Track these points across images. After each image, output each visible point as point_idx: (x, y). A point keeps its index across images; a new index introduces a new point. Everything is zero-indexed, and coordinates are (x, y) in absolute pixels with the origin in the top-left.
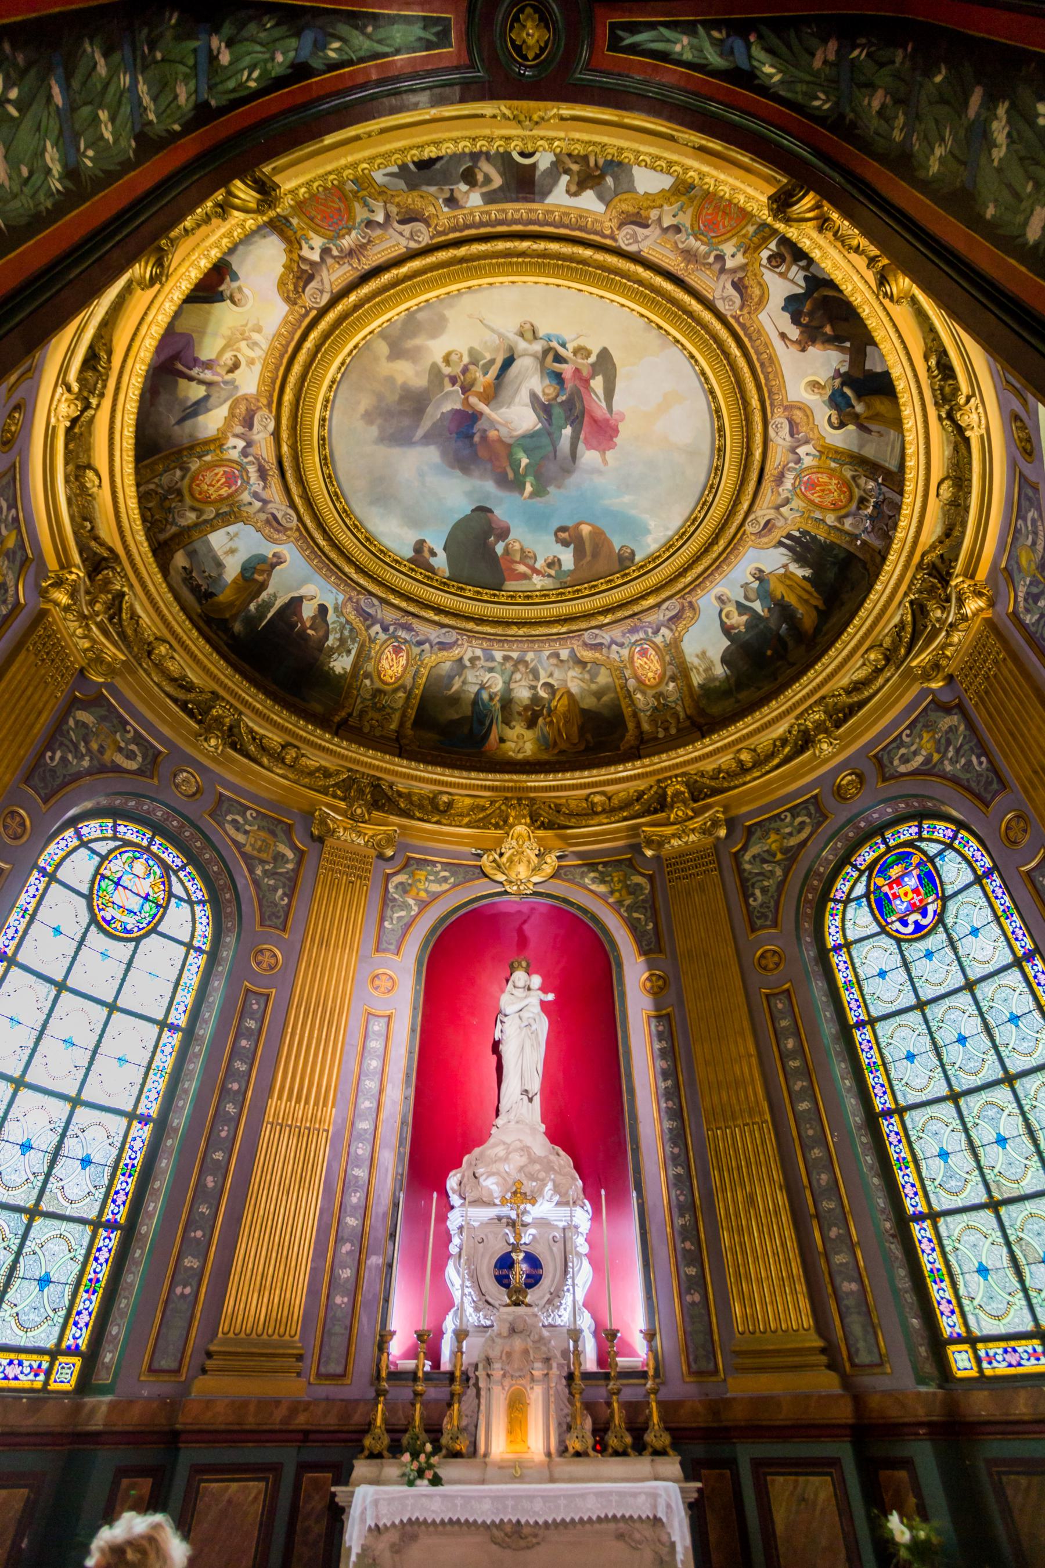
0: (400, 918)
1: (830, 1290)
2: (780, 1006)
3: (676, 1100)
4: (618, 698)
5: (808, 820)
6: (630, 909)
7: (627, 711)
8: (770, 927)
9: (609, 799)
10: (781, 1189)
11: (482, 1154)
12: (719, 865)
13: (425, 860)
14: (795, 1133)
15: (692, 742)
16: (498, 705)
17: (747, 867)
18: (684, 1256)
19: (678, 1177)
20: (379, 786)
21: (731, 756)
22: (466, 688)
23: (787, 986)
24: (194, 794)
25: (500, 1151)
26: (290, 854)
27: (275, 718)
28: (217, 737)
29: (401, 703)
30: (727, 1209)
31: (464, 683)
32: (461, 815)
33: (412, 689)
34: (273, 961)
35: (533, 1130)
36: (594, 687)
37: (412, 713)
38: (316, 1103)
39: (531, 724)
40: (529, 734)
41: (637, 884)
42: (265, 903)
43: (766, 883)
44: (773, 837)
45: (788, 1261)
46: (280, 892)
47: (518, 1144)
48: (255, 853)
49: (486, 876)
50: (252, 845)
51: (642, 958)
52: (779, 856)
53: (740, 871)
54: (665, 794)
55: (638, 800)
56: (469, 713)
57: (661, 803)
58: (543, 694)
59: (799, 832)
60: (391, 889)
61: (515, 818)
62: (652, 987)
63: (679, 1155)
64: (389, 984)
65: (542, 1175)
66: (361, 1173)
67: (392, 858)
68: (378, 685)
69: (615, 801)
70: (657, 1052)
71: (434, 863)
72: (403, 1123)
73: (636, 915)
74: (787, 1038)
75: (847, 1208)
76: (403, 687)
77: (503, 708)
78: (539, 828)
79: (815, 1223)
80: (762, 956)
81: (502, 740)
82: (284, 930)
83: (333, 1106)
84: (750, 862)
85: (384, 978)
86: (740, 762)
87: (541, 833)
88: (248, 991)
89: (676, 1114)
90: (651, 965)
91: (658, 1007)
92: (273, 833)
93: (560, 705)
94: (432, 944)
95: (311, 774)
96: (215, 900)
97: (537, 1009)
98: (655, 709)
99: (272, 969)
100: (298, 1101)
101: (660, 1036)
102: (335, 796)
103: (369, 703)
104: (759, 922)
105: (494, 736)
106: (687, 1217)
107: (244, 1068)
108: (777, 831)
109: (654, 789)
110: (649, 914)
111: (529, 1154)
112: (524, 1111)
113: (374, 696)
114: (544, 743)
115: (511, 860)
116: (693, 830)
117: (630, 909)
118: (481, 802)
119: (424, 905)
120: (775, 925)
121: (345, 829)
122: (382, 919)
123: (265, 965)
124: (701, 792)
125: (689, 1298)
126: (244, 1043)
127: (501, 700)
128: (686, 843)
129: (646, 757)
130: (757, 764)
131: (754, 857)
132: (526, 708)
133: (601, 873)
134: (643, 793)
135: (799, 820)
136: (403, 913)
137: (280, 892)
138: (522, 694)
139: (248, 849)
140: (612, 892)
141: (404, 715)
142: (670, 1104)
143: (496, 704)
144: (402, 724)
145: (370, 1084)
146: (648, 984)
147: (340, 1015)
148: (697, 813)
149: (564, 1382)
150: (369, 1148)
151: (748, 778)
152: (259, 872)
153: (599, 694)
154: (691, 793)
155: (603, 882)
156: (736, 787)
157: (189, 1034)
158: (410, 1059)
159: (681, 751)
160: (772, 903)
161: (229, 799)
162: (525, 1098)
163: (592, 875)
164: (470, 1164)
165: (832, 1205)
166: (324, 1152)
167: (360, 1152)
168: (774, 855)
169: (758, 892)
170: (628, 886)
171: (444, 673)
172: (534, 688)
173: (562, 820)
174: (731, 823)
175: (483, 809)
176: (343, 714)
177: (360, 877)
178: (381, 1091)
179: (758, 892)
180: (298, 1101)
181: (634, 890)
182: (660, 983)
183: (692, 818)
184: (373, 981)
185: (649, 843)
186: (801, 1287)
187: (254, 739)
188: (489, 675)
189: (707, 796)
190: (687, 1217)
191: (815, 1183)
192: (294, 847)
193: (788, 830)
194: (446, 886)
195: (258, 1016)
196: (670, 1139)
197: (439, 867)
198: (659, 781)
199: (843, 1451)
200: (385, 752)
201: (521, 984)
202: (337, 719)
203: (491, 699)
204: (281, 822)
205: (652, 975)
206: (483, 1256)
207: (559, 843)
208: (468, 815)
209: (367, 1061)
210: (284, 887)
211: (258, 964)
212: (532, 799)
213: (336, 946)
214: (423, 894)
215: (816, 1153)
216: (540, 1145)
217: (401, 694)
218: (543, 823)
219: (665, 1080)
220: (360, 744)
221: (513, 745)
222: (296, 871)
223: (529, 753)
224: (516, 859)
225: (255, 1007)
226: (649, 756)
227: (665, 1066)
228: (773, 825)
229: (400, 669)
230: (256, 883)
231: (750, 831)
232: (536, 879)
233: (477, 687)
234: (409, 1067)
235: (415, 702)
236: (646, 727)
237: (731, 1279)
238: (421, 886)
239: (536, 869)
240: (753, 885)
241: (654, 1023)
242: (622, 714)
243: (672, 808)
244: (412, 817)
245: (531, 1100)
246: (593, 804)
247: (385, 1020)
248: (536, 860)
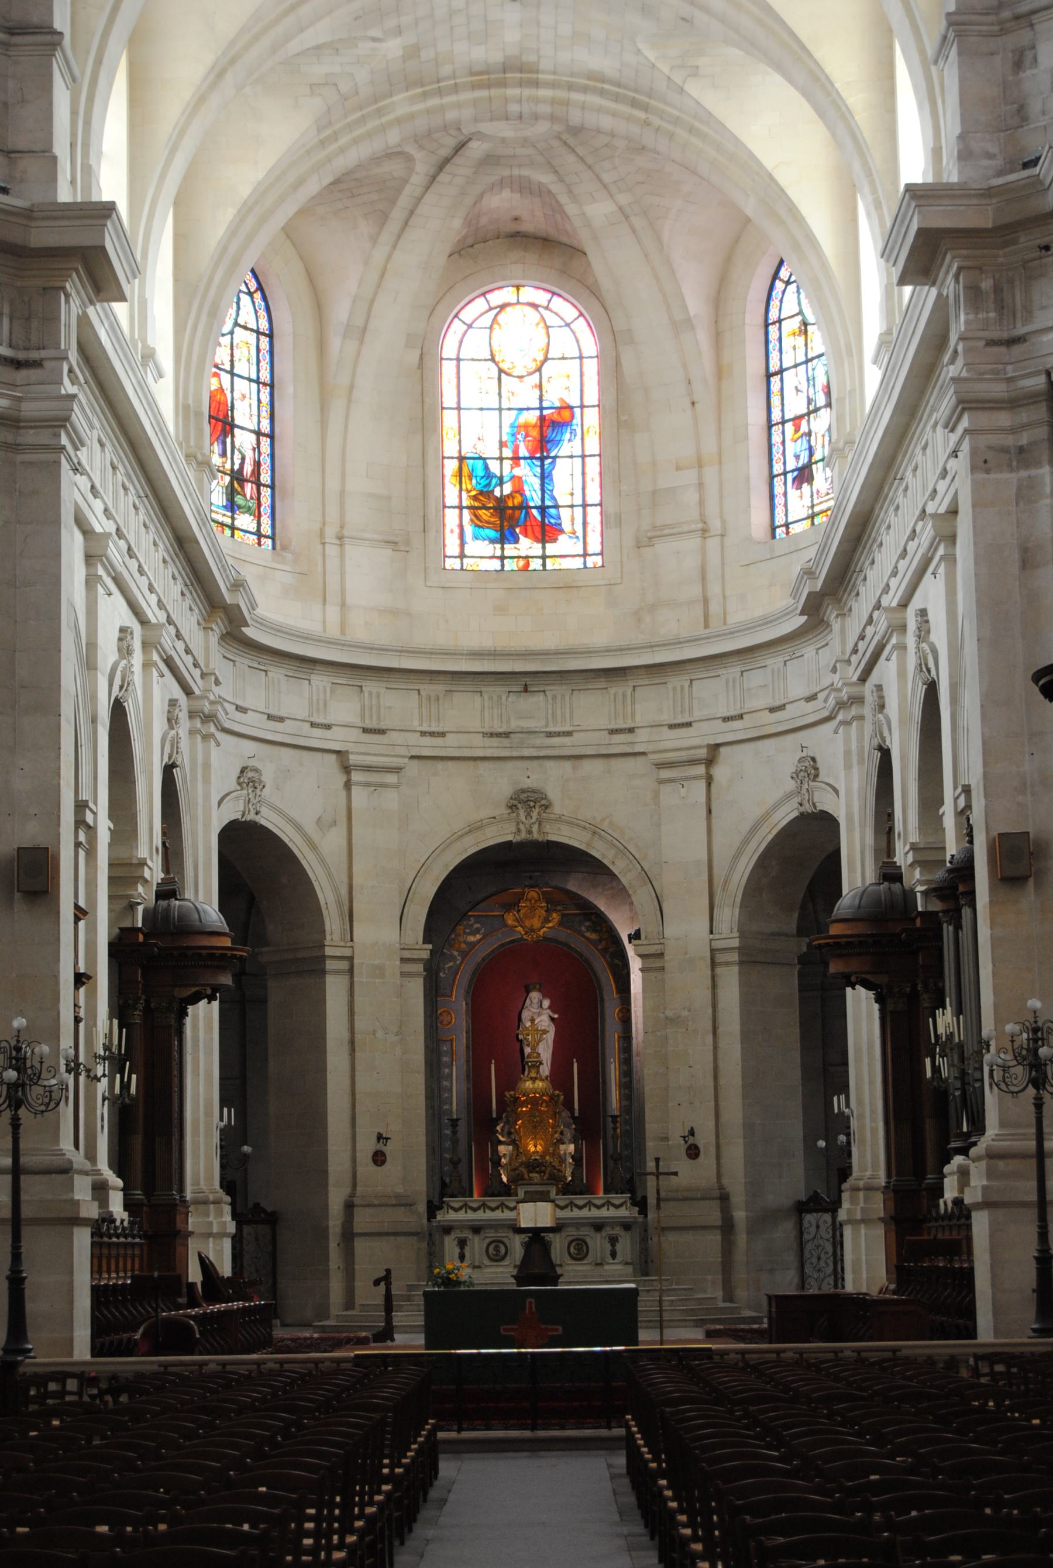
0: (449, 968)
72: (468, 1104)
73: (616, 961)
119: (464, 954)
136: (451, 964)
140: (600, 940)
146: (620, 1015)
155: (595, 931)
163: (587, 924)
197: (472, 920)
214: (463, 946)
239: (547, 920)
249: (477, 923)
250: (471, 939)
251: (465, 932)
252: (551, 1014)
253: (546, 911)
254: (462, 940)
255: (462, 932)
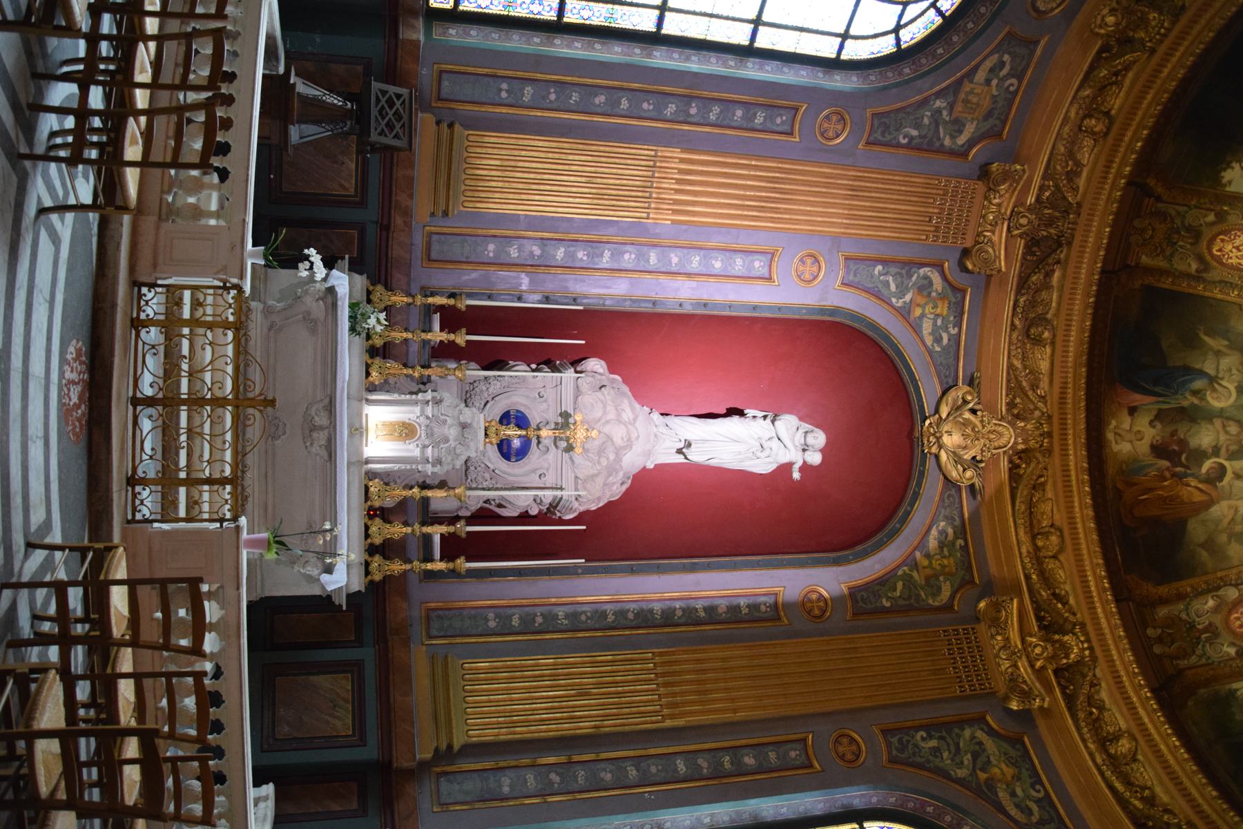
0: (887, 284)
1: (502, 764)
2: (793, 754)
3: (682, 621)
4: (1206, 573)
5: (1034, 819)
6: (907, 579)
7: (1186, 586)
8: (889, 753)
9: (1055, 557)
10: (595, 727)
11: (624, 394)
12: (967, 698)
13: (962, 313)
14: (652, 751)
15: (1143, 673)
16: (1185, 404)
17: (967, 733)
18: (528, 615)
19: (604, 614)
20: (1060, 245)
21: (1123, 725)
22: (1210, 356)
23: (816, 765)
24: (1036, 9)
25: (627, 415)
26: (962, 140)
27: (1149, 97)
28: (1117, 24)
29: (1179, 266)
30: (573, 665)
31: (1218, 354)
32: (1024, 359)
33: (1204, 280)
34: (831, 134)
35: (648, 454)
36: (1223, 538)
37: (1167, 283)
38: (676, 202)
39: (1159, 450)
40: (1143, 447)
41: (939, 589)
42: (901, 115)
43: (946, 755)
44: (1009, 771)
45: (527, 723)
46: (914, 133)
47: (634, 435)
48: (962, 96)
49: (944, 393)
50: (971, 92)
51: (846, 591)
52: (983, 776)
53: (961, 723)
54: (1065, 633)
55: (1054, 594)
56: (1170, 364)
57: (1051, 627)
58: (1207, 465)
59: (1017, 806)
60: (922, 271)
61: (1023, 429)
62: (811, 601)
63: (626, 618)
64: (807, 276)
65: (604, 462)
66: (606, 260)
67: (966, 270)
68: (1207, 234)
69: (1051, 565)
70: (735, 602)
71: (959, 324)
72: (654, 303)
73: (900, 585)
74: (754, 757)
75: (579, 796)
76: (1205, 266)
77: (1182, 411)
78: (1011, 461)
79: (563, 759)
80: (853, 740)
81: (1132, 411)
82: (868, 143)
83: (673, 222)
84: (973, 737)
85: (815, 269)
86: (1116, 738)
87: (1004, 464)
88: (796, 109)
89: (668, 618)
90: (837, 601)
91: (788, 606)
92: (989, 115)
93: (1192, 491)
94: (856, 325)
95: (1071, 155)
96: (901, 56)
97: (784, 459)
98: (1192, 626)
99: (822, 135)
100: (679, 181)
101: (754, 607)
102: (1042, 189)
103: (1178, 222)
104: (895, 740)
105: (1138, 399)
106: (566, 622)
107: (712, 117)
108: (1018, 778)
109: (1072, 618)
110: (901, 602)
111: (624, 448)
112: (668, 444)
113: (1189, 229)
114: (1131, 469)
115: (966, 423)
116: (1015, 666)
117: (907, 579)
118: (1044, 383)
119: (904, 313)
120: (892, 760)
121: (999, 205)
122: (884, 262)
123: (826, 125)
124: (1069, 681)
125: (491, 615)
126: (739, 113)
127: (1194, 406)
128: (997, 656)
129: (1118, 607)
130: (1113, 761)
131: (980, 743)
132: (1183, 443)
133: (953, 543)
134: (1065, 604)
135: (1035, 808)
136: (893, 287)
137: (914, 133)
138: (1204, 437)
139: (967, 87)
141: (1162, 272)
142: (679, 613)
143: (1188, 400)
144: (1149, 271)
145: (695, 262)
146: (814, 596)
147: (772, 220)
148: (1040, 673)
149: (421, 481)
150: (630, 266)
151: (1092, 746)
152: (938, 103)
153: (1210, 545)
154: (1068, 667)
155: (941, 545)
156: (1078, 729)
157: (748, 52)
158: (723, 306)
159: (1129, 656)
160: (919, 760)
161: (1032, 53)
162: (681, 445)
163: (950, 531)
164: (613, 381)
165: (581, 780)
166: (626, 217)
167: (627, 256)
168: (983, 770)
169: (933, 743)
170: (936, 576)
171: (1232, 323)
172: (1216, 451)
173: (1022, 492)
174: (1025, 717)
175: (1034, 387)
176: (1160, 190)
177: (937, 228)
178: (689, 275)
179: (933, 743)
180: (679, 181)
181: (932, 584)
182: (817, 612)
183: (1032, 666)
184: (811, 256)
185: (997, 607)
186: (504, 735)
187: (1116, 74)
188: (1232, 388)
189: (1063, 689)
190: (566, 622)
191: (602, 765)
192: (971, 143)
193: (1019, 791)
194: (929, 341)
195: (769, 125)
196: (642, 610)
197: (954, 331)
198: (1083, 625)
199: (370, 752)
200: (1107, 250)
201: (810, 440)
202: (1151, 182)
203: (1195, 393)
204: (1004, 123)
205: (825, 600)
206: (527, 397)
207: (990, 490)
208: (1025, 368)
209: (720, 256)
210: (920, 136)
211: (827, 117)
212: (1050, 451)
213: (851, 207)
214: (918, 312)
215: (633, 773)
216: (634, 461)
217: (1194, 266)
218: (1018, 466)
219: (705, 609)
220: (1117, 214)
221: (1126, 426)
222: (942, 150)
223: (1116, 448)
224: (969, 431)
225: (779, 120)
226: (1120, 612)
227: (720, 611)
228: (1025, 773)
229: (1234, 261)
230: (924, 103)
231: (1016, 741)
232: (944, 456)
233: (1212, 372)
234: (716, 305)
235: (1184, 286)
236: (1163, 612)
237: (510, 661)
238: (928, 309)
239: (958, 459)
240: (942, 738)
241: (771, 600)
242: (1180, 578)
243: (1045, 640)
244: (1018, 293)
245: (680, 451)
246: (1046, 535)
247: (767, 275)
248: (967, 457)
249: (949, 340)
250: (927, 327)
251: (938, 315)
252: (796, 467)
253: (974, 458)
254: (928, 309)
255: (938, 311)
